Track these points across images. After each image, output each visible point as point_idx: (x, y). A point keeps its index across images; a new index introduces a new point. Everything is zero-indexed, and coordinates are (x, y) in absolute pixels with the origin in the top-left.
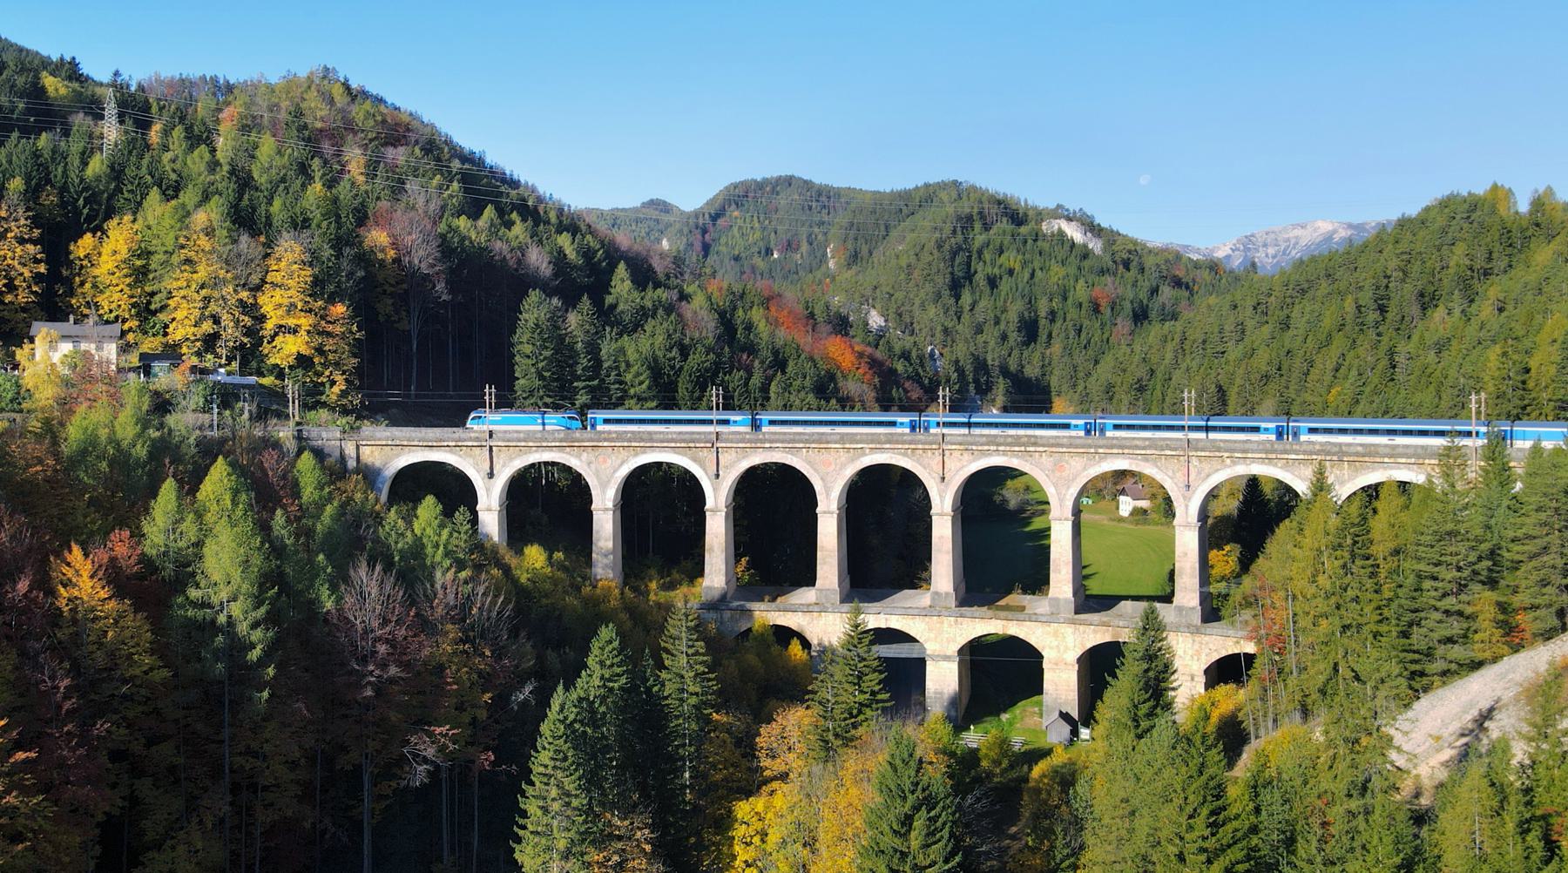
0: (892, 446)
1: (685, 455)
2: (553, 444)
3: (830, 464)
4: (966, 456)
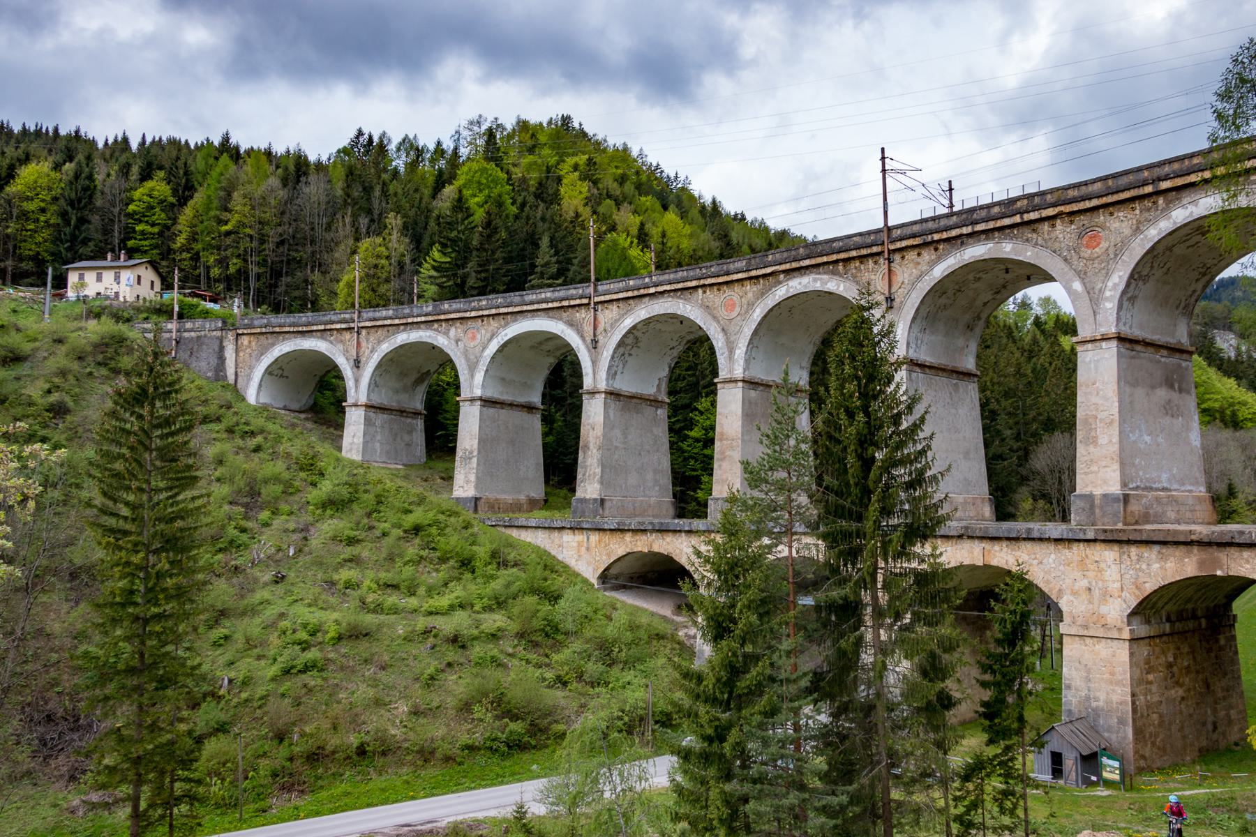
0: (813, 262)
1: (561, 319)
2: (419, 319)
3: (734, 305)
4: (927, 255)
